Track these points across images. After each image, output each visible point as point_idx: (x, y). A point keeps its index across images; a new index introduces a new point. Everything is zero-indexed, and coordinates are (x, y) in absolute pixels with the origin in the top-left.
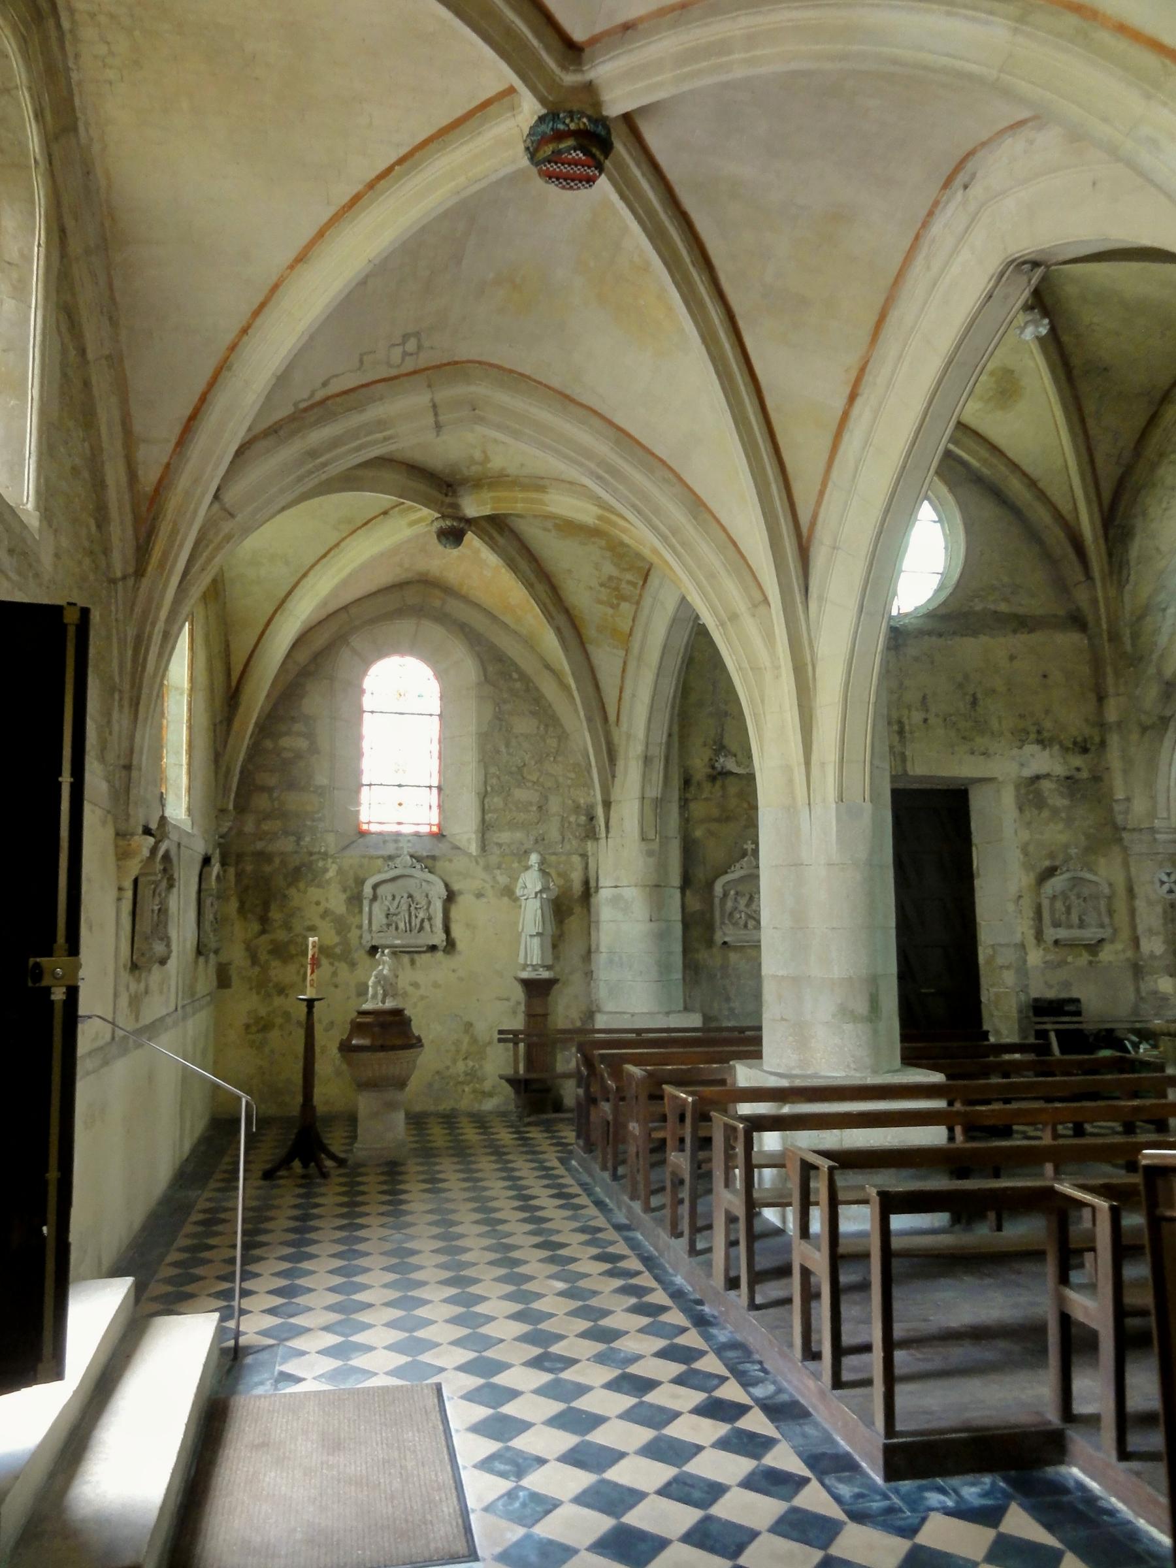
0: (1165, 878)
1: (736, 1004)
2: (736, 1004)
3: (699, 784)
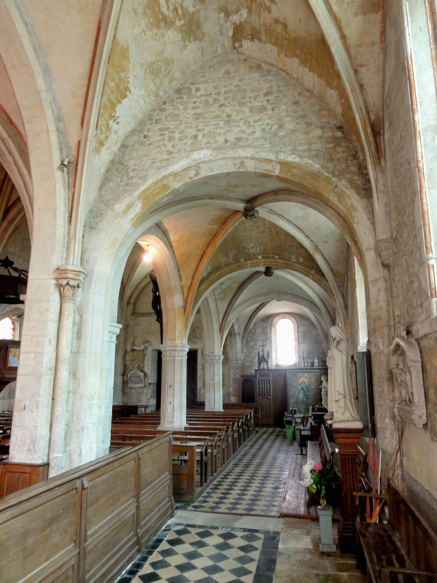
0: (234, 372)
1: (132, 401)
2: (132, 401)
3: (129, 352)
